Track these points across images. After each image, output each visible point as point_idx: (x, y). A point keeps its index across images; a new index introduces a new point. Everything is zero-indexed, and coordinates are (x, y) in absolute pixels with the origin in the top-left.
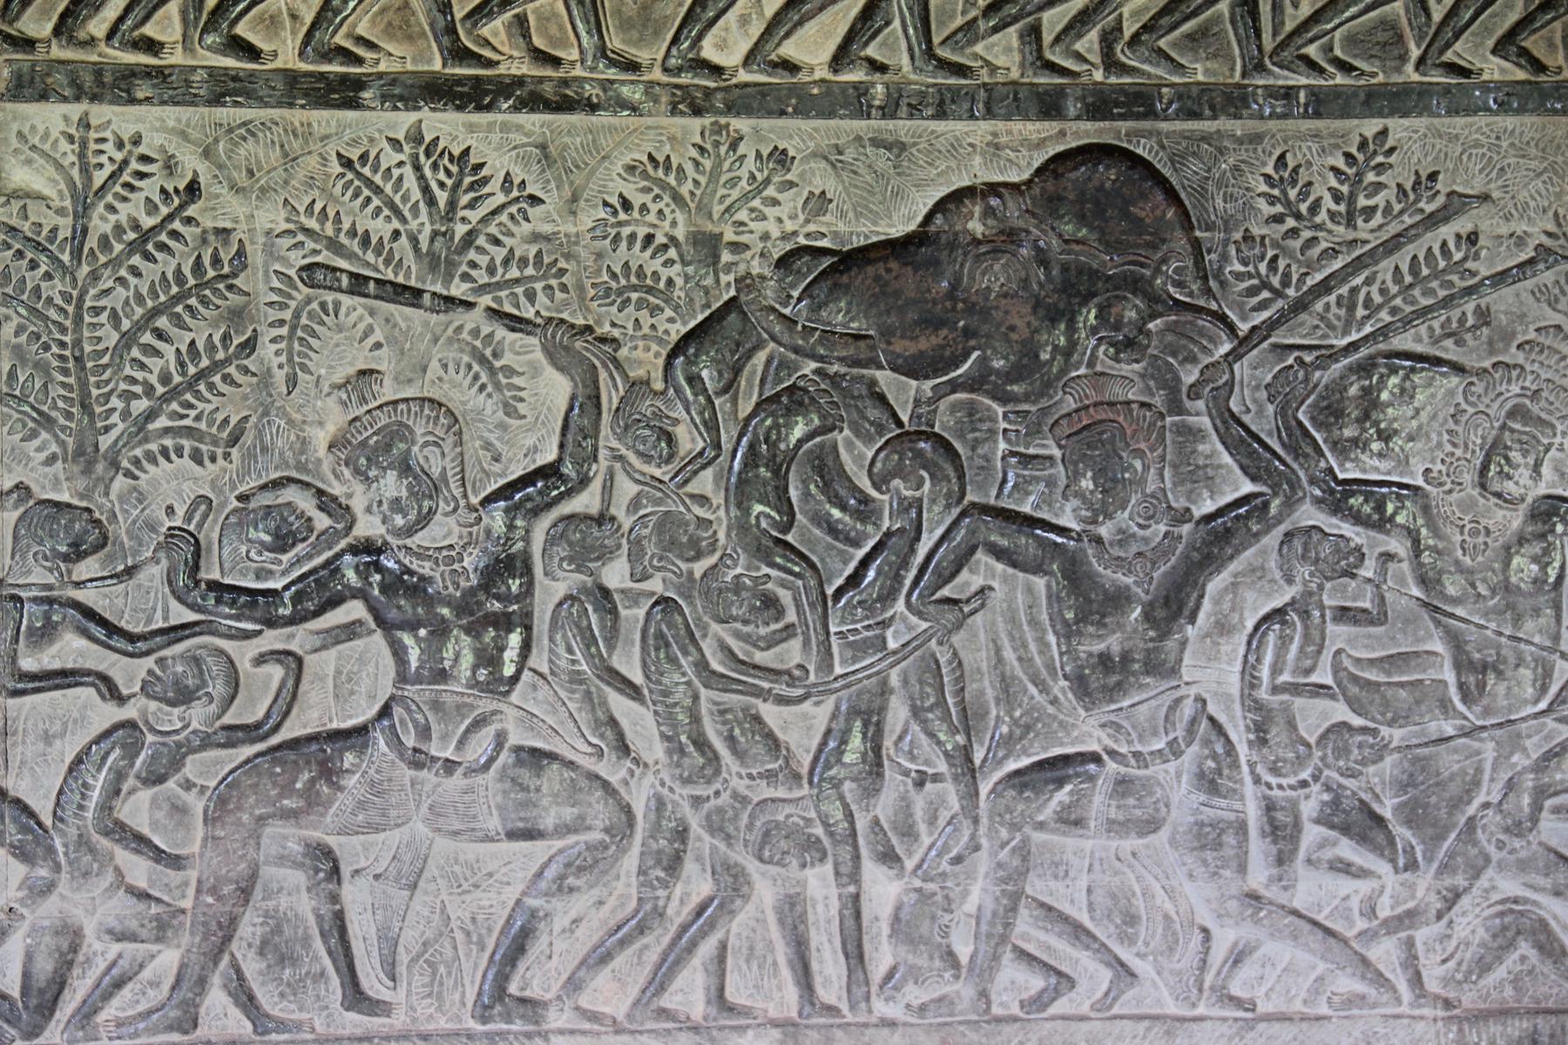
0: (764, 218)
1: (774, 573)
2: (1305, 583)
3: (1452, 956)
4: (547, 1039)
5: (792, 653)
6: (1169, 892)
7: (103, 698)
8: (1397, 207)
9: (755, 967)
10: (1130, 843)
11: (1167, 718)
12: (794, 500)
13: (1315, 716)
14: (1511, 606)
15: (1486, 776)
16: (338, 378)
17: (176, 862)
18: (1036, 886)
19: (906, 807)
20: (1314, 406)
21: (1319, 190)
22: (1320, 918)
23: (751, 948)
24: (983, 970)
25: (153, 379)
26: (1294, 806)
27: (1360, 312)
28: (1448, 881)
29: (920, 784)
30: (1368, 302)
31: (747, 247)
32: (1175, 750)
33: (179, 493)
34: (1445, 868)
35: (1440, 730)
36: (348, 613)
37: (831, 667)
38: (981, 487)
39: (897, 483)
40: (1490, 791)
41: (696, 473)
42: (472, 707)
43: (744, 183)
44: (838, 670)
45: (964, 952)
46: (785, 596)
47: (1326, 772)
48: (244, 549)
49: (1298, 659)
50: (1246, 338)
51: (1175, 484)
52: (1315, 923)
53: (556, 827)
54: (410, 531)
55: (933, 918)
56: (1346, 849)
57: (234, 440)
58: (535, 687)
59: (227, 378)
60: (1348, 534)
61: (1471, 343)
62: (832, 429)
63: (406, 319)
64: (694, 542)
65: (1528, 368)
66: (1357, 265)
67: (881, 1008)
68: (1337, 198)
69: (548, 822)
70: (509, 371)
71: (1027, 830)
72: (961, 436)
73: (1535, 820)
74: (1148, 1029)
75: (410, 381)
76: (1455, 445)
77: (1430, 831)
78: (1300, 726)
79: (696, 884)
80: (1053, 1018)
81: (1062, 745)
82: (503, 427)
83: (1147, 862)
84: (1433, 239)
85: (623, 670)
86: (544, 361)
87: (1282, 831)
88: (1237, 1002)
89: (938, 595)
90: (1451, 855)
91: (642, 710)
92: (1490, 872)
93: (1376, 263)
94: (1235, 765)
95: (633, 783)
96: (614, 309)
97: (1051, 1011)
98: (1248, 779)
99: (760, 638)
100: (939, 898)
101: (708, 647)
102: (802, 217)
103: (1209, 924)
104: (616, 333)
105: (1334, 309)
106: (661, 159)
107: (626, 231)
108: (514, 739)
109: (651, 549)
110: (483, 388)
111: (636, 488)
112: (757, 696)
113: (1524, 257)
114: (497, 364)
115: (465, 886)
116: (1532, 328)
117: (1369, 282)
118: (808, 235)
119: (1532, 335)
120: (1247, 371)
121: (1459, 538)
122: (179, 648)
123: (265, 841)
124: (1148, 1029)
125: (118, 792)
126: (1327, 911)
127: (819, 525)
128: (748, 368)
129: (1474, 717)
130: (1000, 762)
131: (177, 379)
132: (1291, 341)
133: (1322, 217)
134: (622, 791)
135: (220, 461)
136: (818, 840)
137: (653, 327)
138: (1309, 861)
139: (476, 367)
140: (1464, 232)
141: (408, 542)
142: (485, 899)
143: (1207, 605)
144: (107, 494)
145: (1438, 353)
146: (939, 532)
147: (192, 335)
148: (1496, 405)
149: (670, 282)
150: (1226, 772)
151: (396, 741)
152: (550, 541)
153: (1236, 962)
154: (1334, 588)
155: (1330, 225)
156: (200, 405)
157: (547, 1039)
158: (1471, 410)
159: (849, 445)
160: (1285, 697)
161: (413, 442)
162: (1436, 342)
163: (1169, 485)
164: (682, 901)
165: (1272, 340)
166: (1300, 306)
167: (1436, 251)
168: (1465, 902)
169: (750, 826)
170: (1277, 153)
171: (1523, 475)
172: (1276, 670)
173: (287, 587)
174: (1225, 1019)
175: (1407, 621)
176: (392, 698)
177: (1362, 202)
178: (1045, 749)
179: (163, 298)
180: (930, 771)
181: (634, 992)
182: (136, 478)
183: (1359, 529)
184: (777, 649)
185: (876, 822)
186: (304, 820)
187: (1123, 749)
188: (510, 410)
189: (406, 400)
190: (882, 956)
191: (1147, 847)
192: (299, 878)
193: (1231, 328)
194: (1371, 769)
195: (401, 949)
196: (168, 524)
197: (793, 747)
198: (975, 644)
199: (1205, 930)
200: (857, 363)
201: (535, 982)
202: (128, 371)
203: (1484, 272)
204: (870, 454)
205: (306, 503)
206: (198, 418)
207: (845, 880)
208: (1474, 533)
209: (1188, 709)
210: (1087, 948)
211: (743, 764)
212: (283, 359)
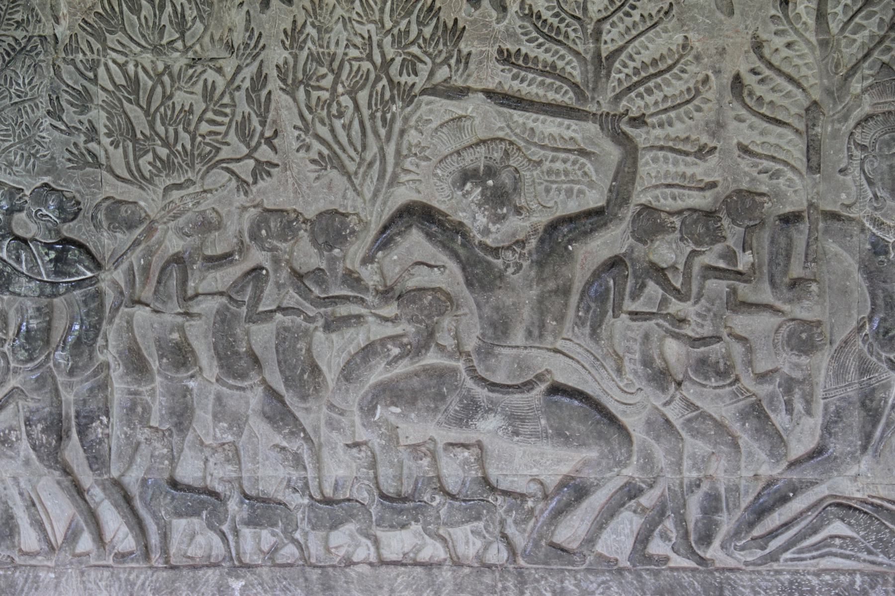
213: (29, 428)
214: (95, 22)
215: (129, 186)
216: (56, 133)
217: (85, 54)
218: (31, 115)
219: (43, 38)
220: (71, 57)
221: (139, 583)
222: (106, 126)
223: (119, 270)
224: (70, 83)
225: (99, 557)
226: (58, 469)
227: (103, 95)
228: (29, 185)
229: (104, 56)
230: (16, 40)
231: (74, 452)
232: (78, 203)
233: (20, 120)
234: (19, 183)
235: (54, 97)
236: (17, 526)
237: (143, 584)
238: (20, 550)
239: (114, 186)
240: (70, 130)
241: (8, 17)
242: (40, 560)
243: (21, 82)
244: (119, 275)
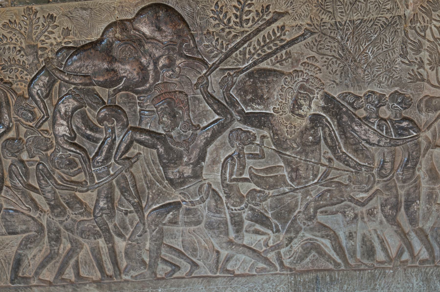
0: (50, 38)
1: (71, 153)
2: (238, 147)
3: (292, 256)
4: (31, 289)
6: (206, 241)
8: (256, 19)
10: (193, 228)
11: (199, 191)
12: (75, 130)
13: (245, 188)
14: (304, 150)
15: (300, 203)
18: (166, 241)
20: (236, 88)
21: (230, 14)
22: (252, 247)
24: (152, 267)
26: (240, 215)
27: (248, 56)
28: (289, 235)
29: (126, 214)
30: (250, 52)
31: (46, 48)
32: (203, 201)
34: (288, 231)
35: (284, 190)
37: (94, 181)
38: (134, 122)
39: (105, 122)
40: (300, 208)
41: (42, 123)
43: (41, 27)
45: (147, 260)
47: (249, 205)
49: (237, 171)
50: (211, 68)
51: (194, 118)
52: (250, 248)
53: (21, 231)
55: (136, 252)
56: (258, 227)
60: (250, 130)
61: (286, 64)
62: (82, 107)
65: (305, 72)
66: (244, 41)
67: (124, 277)
68: (236, 17)
71: (160, 226)
73: (315, 216)
74: (202, 281)
76: (282, 99)
77: (283, 221)
78: (241, 191)
79: (65, 246)
80: (174, 278)
81: (169, 200)
83: (198, 233)
84: (269, 29)
85: (33, 184)
87: (238, 224)
88: (228, 271)
89: (123, 157)
90: (290, 227)
92: (303, 231)
93: (251, 39)
94: (222, 203)
95: (41, 217)
96: (8, 72)
97: (175, 276)
98: (226, 208)
99: (71, 173)
100: (136, 246)
102: (62, 37)
103: (219, 249)
104: (11, 80)
105: (239, 56)
106: (13, 21)
107: (7, 46)
111: (26, 130)
112: (73, 191)
113: (301, 33)
116: (305, 57)
117: (249, 45)
118: (65, 43)
119: (306, 60)
120: (213, 79)
121: (286, 130)
124: (202, 281)
126: (254, 245)
127: (84, 137)
129: (294, 186)
130: (150, 206)
132: (227, 67)
133: (232, 24)
134: (39, 220)
136: (98, 231)
137: (22, 77)
138: (246, 231)
140: (280, 26)
142: (8, 251)
143: (208, 155)
145: (275, 68)
146: (121, 137)
148: (295, 85)
149: (23, 61)
150: (219, 206)
153: (227, 261)
154: (247, 148)
155: (235, 26)
157: (31, 289)
158: (287, 87)
159: (90, 112)
160: (235, 183)
162: (273, 65)
163: (192, 117)
164: (64, 249)
165: (220, 67)
166: (227, 56)
167: (271, 33)
168: (295, 240)
169: (77, 229)
170: (215, 2)
171: (305, 108)
172: (231, 175)
174: (225, 277)
175: (271, 157)
177: (245, 17)
178: (164, 202)
180: (129, 210)
181: (54, 274)
183: (253, 128)
184: (78, 175)
185: (115, 226)
187: (187, 201)
190: (124, 263)
191: (198, 228)
193: (206, 64)
194: (264, 203)
197: (88, 204)
198: (138, 170)
199: (218, 252)
200: (86, 85)
203: (288, 39)
207: (108, 242)
208: (291, 128)
209: (205, 187)
210: (182, 259)
211: (72, 211)
213: (383, 208)
214: (427, 6)
215: (437, 89)
216: (403, 65)
217: (421, 23)
218: (392, 57)
219: (400, 17)
220: (414, 25)
221: (430, 273)
222: (428, 60)
223: (429, 131)
224: (412, 39)
225: (412, 262)
226: (395, 225)
227: (428, 44)
228: (388, 92)
229: (430, 24)
230: (387, 19)
231: (402, 217)
232: (412, 99)
233: (386, 60)
234: (383, 91)
235: (404, 47)
236: (375, 251)
237: (432, 273)
238: (377, 261)
239: (430, 90)
240: (410, 63)
241: (383, 7)
242: (386, 265)
243: (388, 40)
244: (429, 134)
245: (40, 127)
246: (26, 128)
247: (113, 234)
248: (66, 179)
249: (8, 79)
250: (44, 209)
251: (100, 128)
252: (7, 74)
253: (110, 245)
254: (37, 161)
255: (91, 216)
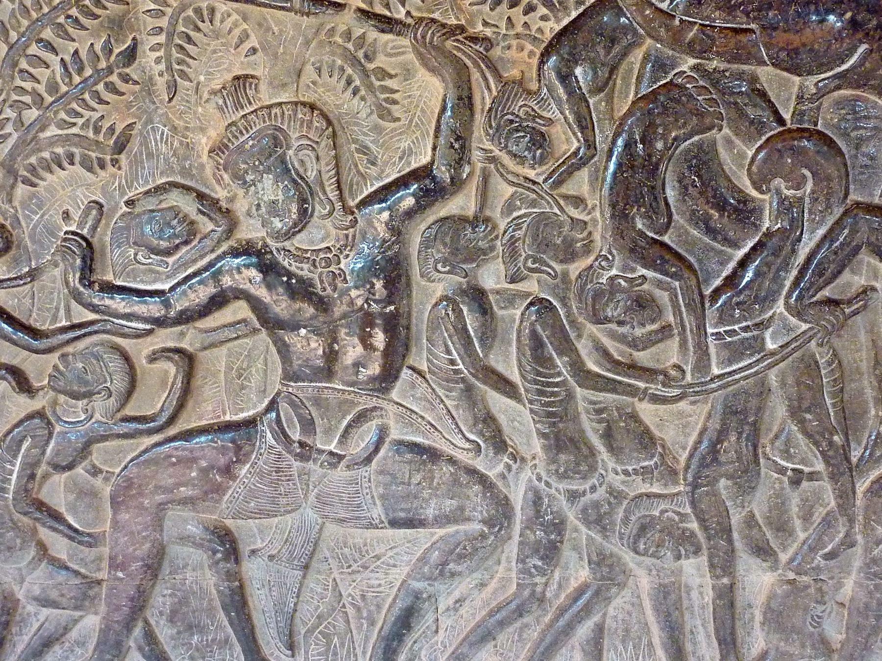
5: (670, 354)
7: (14, 389)
9: (631, 647)
12: (671, 201)
16: (216, 85)
17: (93, 541)
19: (779, 506)
23: (627, 631)
25: (41, 89)
29: (796, 482)
33: (74, 199)
36: (235, 312)
41: (570, 173)
42: (353, 404)
44: (716, 371)
46: (663, 297)
48: (132, 252)
53: (436, 518)
54: (289, 235)
55: (806, 609)
57: (120, 147)
58: (413, 386)
59: (112, 88)
62: (710, 129)
63: (278, 23)
64: (569, 244)
69: (430, 512)
70: (384, 74)
72: (845, 135)
75: (284, 85)
82: (377, 129)
85: (500, 368)
86: (417, 63)
91: (520, 407)
95: (510, 477)
96: (486, 8)
100: (812, 590)
101: (583, 347)
104: (488, 32)
108: (395, 433)
109: (525, 250)
110: (355, 92)
111: (511, 190)
114: (371, 66)
115: (354, 567)
122: (81, 345)
123: (167, 523)
125: (32, 477)
128: (623, 67)
131: (64, 89)
134: (500, 484)
135: (111, 169)
136: (693, 534)
139: (349, 71)
141: (287, 244)
144: (10, 201)
146: (821, 232)
147: (76, 45)
151: (282, 435)
152: (427, 243)
156: (87, 114)
159: (728, 142)
161: (289, 147)
164: (560, 586)
169: (626, 520)
173: (173, 289)
176: (278, 394)
179: (46, 10)
180: (807, 469)
182: (34, 185)
186: (201, 505)
188: (385, 114)
189: (280, 104)
192: (199, 556)
195: (297, 621)
196: (66, 229)
200: (736, 58)
201: (423, 653)
202: (18, 82)
204: (750, 154)
205: (189, 206)
206: (85, 125)
207: (719, 571)
211: (619, 461)
212: (162, 67)
245: (559, 183)
246: (513, 184)
247: (738, 544)
248: (617, 357)
249: (480, 27)
250: (524, 451)
251: (753, 200)
252: (480, 12)
253: (725, 580)
254: (528, 294)
255: (676, 483)
